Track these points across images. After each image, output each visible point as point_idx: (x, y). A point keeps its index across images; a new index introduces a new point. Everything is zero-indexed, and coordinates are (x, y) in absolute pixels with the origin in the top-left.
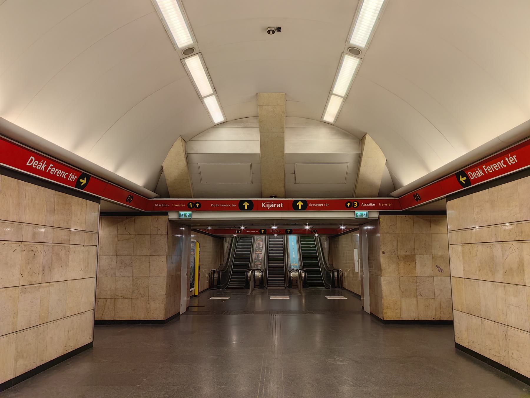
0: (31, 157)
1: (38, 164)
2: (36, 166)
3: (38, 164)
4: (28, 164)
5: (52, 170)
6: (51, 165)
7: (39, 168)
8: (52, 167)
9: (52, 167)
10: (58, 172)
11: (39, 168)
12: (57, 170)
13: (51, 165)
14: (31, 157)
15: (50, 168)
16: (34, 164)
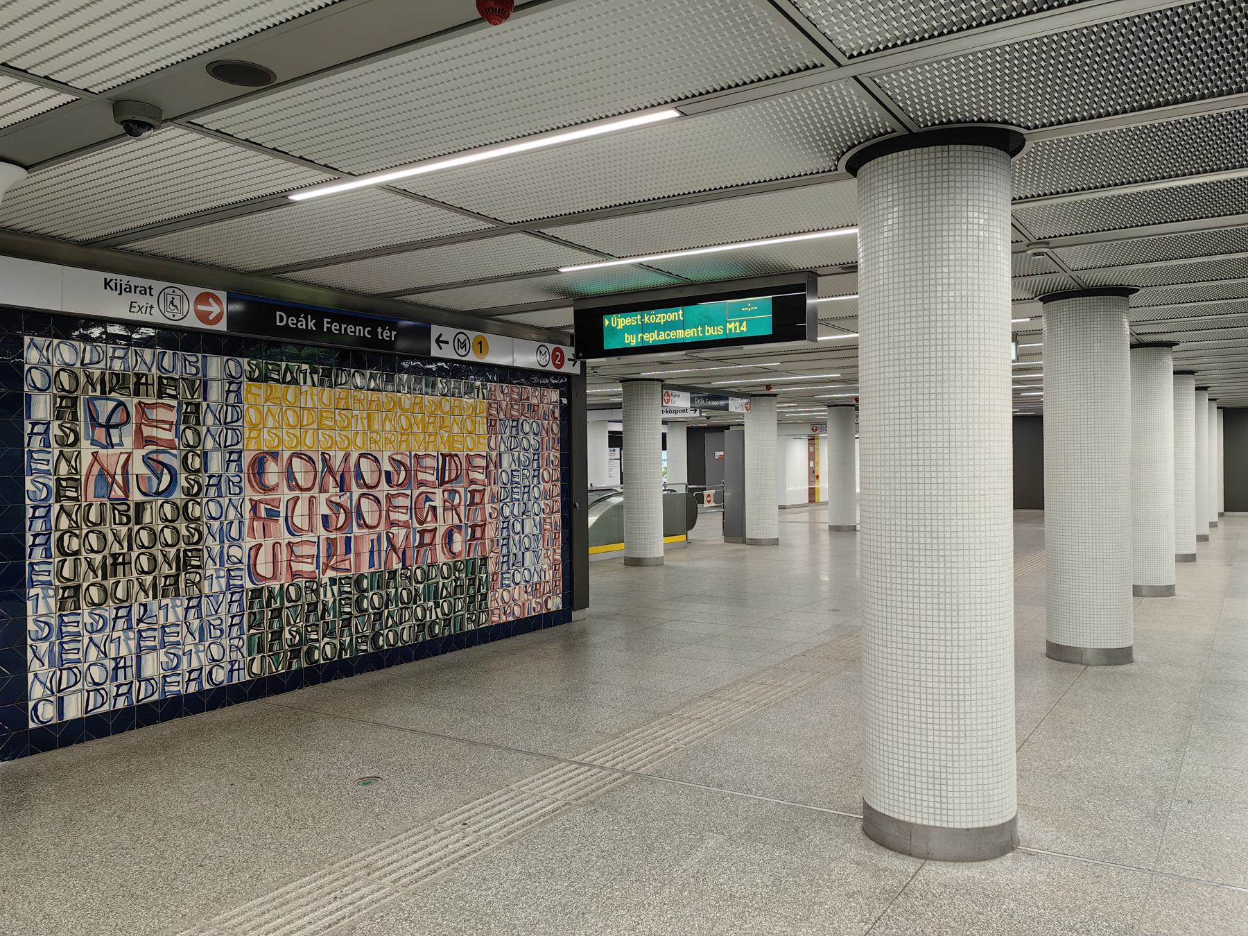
0: (278, 313)
1: (298, 321)
2: (296, 324)
3: (298, 321)
4: (278, 324)
5: (333, 328)
6: (325, 320)
7: (304, 327)
8: (328, 323)
9: (328, 323)
10: (349, 330)
11: (304, 327)
12: (343, 326)
13: (325, 320)
14: (278, 313)
15: (326, 325)
16: (290, 322)
